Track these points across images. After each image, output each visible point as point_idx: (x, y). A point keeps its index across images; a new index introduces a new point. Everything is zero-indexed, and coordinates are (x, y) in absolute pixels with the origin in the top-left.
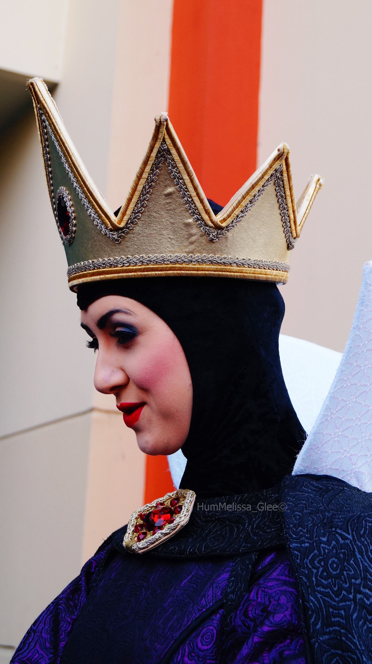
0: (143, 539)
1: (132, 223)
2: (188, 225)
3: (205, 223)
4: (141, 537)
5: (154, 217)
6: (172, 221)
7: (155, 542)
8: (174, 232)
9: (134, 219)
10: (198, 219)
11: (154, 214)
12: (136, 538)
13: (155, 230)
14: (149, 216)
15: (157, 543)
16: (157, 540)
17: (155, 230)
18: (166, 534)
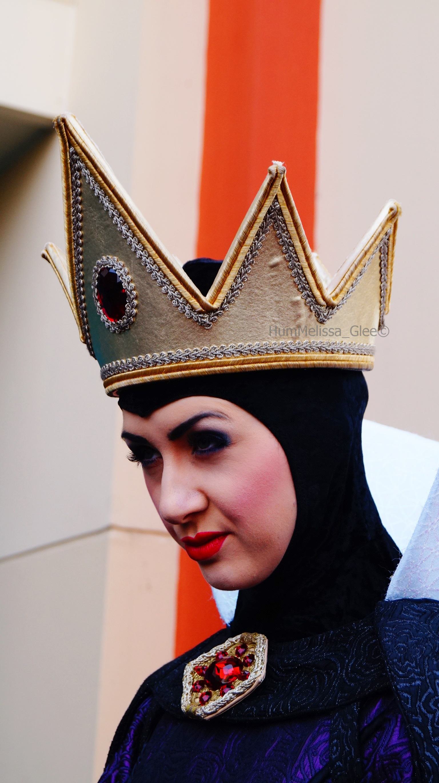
0: (207, 701)
1: (229, 302)
2: (296, 304)
3: (316, 300)
4: (205, 698)
5: (256, 295)
6: (277, 298)
7: (225, 705)
8: (280, 312)
9: (231, 297)
10: (309, 296)
11: (257, 291)
12: (198, 700)
13: (257, 311)
14: (250, 294)
15: (228, 706)
16: (228, 702)
17: (257, 311)
18: (238, 694)
